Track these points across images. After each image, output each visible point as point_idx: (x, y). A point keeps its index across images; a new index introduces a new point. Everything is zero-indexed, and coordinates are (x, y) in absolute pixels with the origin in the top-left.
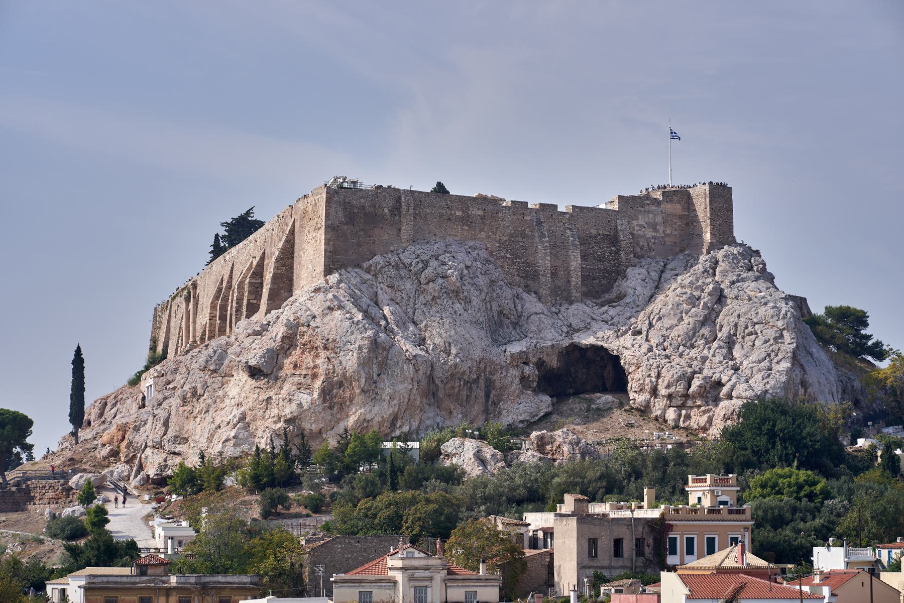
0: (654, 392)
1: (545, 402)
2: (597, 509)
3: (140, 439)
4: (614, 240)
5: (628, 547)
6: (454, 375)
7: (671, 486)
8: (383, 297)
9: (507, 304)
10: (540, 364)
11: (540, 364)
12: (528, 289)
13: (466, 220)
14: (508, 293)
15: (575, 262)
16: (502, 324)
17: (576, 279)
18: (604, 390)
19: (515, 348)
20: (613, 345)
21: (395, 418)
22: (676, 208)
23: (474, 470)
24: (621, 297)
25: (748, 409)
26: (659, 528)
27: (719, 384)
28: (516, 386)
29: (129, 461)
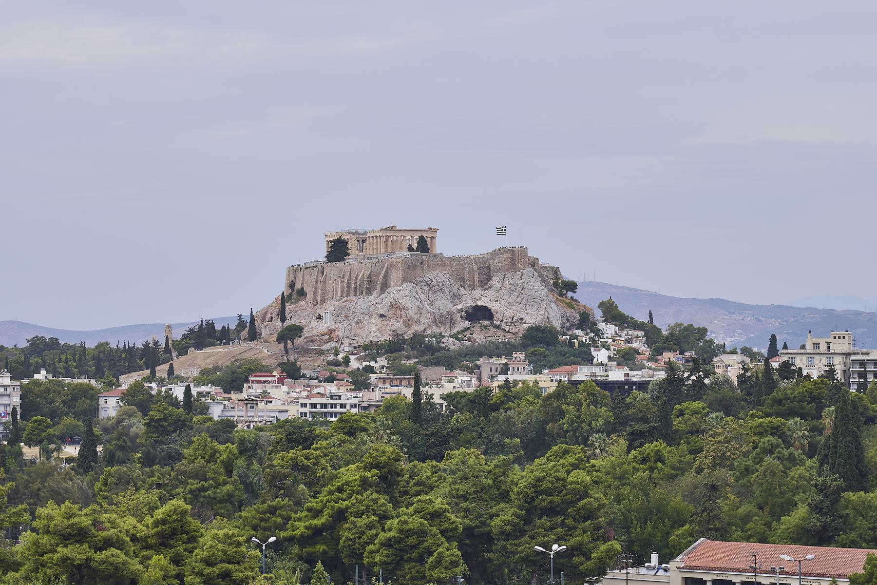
0: (502, 321)
1: (467, 324)
2: (491, 360)
3: (340, 334)
4: (488, 268)
5: (499, 370)
6: (442, 316)
7: (509, 356)
8: (419, 292)
9: (455, 291)
10: (466, 312)
11: (466, 312)
12: (461, 286)
13: (443, 265)
14: (456, 287)
15: (476, 276)
16: (455, 297)
17: (476, 282)
18: (485, 319)
19: (459, 307)
20: (489, 306)
21: (425, 329)
22: (508, 255)
23: (452, 347)
24: (491, 287)
25: (530, 329)
26: (506, 365)
27: (522, 319)
28: (459, 319)
29: (337, 341)
